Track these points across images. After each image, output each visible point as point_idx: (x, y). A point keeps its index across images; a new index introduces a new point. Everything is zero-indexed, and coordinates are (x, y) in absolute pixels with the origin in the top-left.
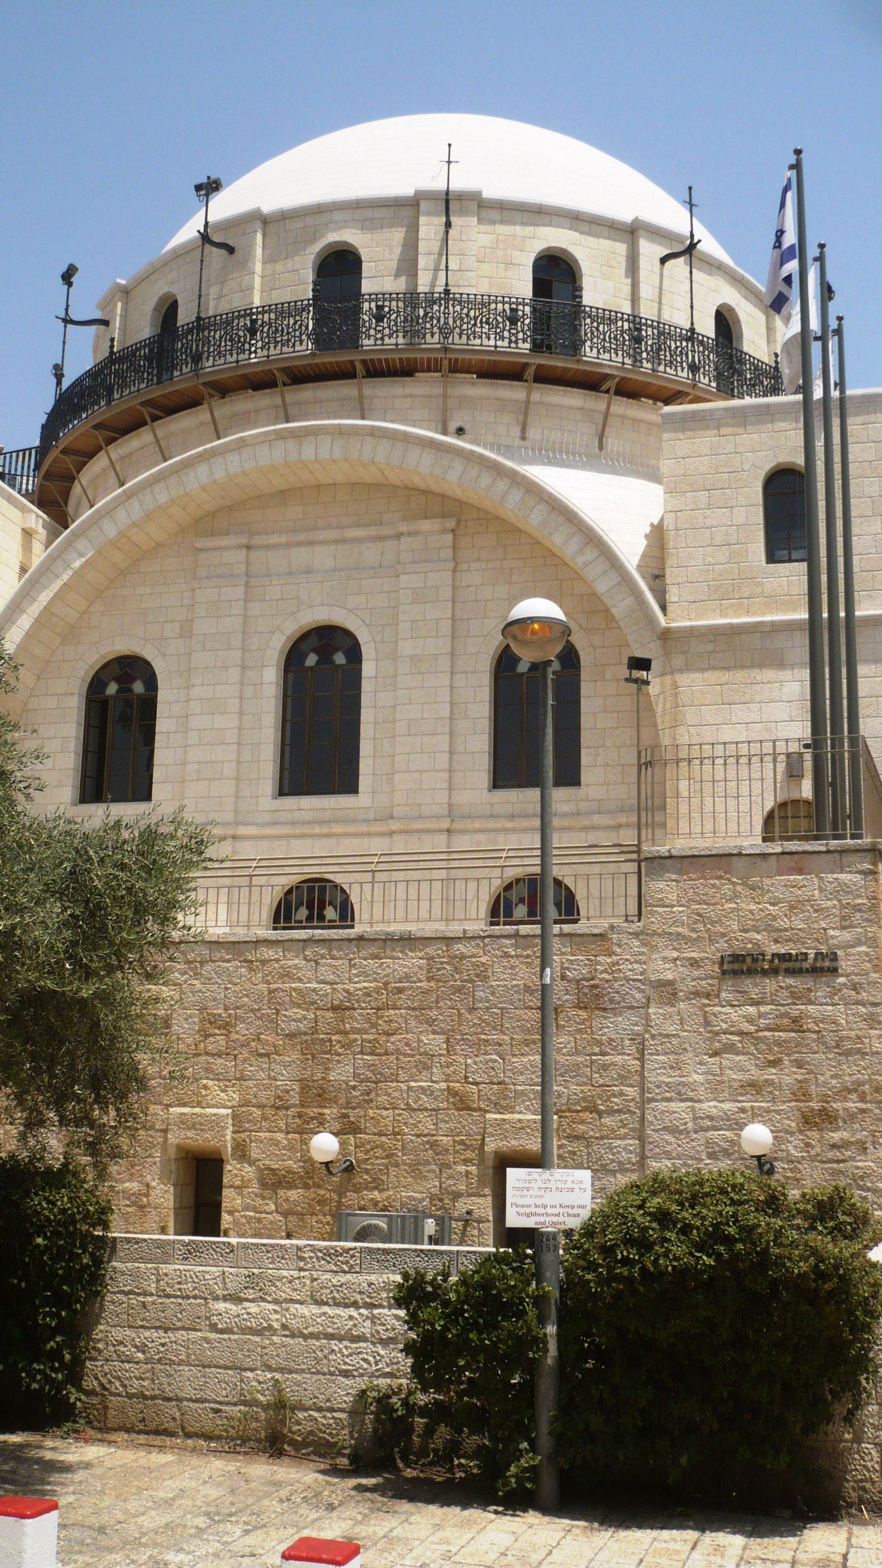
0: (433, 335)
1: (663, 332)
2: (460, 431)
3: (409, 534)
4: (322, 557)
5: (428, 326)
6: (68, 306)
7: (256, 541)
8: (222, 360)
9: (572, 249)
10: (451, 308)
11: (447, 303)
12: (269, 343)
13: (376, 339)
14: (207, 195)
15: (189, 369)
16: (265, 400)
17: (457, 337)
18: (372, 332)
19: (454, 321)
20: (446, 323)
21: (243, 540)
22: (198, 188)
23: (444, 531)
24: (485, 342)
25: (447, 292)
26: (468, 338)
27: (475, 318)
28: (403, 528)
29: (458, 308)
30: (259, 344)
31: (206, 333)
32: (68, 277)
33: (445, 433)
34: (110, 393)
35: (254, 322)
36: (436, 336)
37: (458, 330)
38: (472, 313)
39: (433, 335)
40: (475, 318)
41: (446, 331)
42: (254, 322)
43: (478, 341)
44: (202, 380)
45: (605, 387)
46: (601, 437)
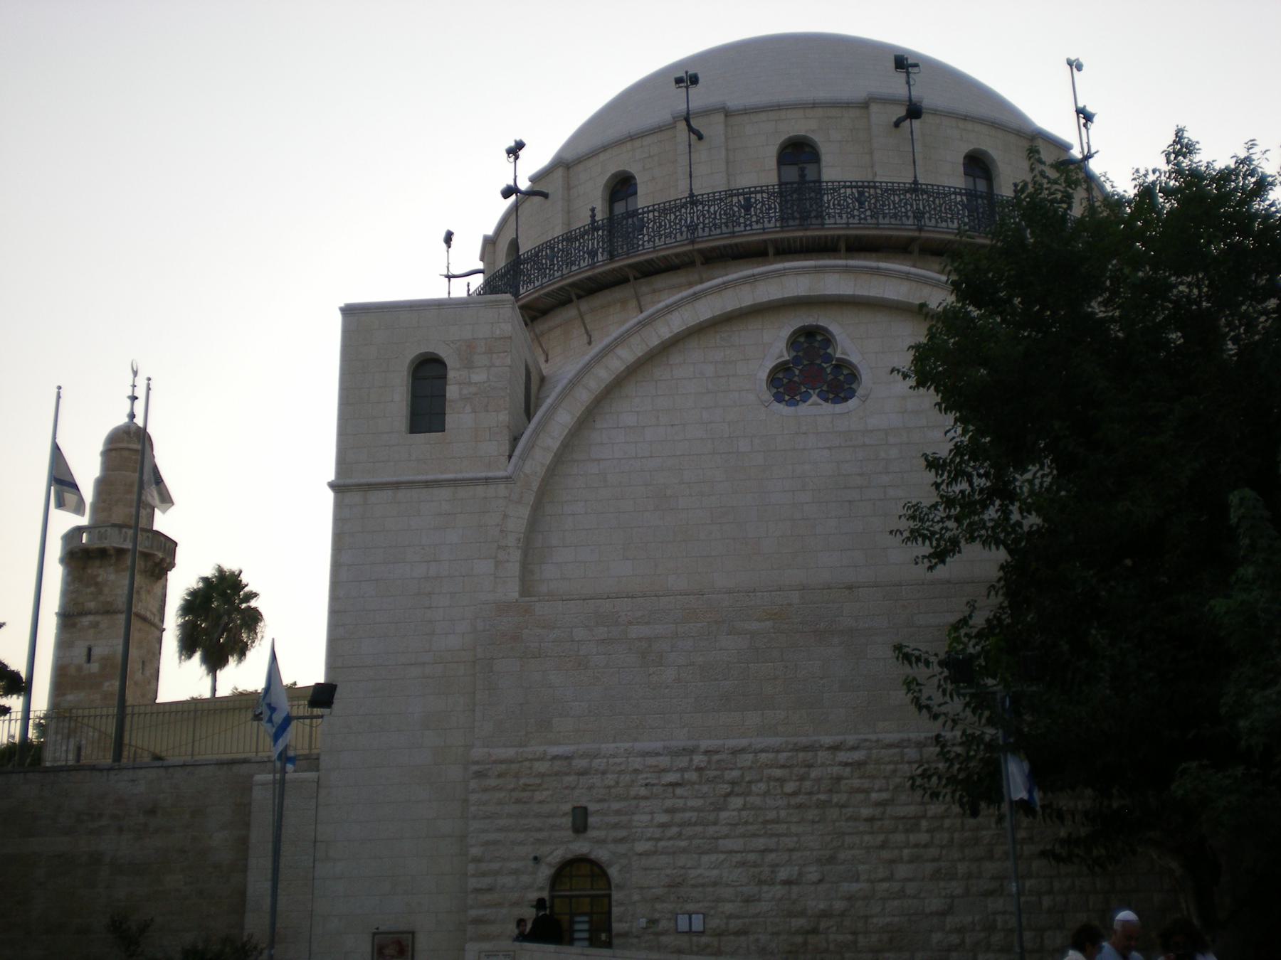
0: (908, 218)
8: (718, 231)
14: (687, 87)
15: (684, 236)
18: (856, 213)
22: (679, 81)
24: (950, 225)
25: (915, 182)
27: (940, 206)
30: (754, 219)
31: (700, 207)
32: (515, 150)
34: (593, 254)
35: (747, 200)
37: (927, 215)
39: (908, 218)
40: (940, 206)
41: (919, 215)
42: (747, 200)
43: (944, 224)
44: (697, 246)
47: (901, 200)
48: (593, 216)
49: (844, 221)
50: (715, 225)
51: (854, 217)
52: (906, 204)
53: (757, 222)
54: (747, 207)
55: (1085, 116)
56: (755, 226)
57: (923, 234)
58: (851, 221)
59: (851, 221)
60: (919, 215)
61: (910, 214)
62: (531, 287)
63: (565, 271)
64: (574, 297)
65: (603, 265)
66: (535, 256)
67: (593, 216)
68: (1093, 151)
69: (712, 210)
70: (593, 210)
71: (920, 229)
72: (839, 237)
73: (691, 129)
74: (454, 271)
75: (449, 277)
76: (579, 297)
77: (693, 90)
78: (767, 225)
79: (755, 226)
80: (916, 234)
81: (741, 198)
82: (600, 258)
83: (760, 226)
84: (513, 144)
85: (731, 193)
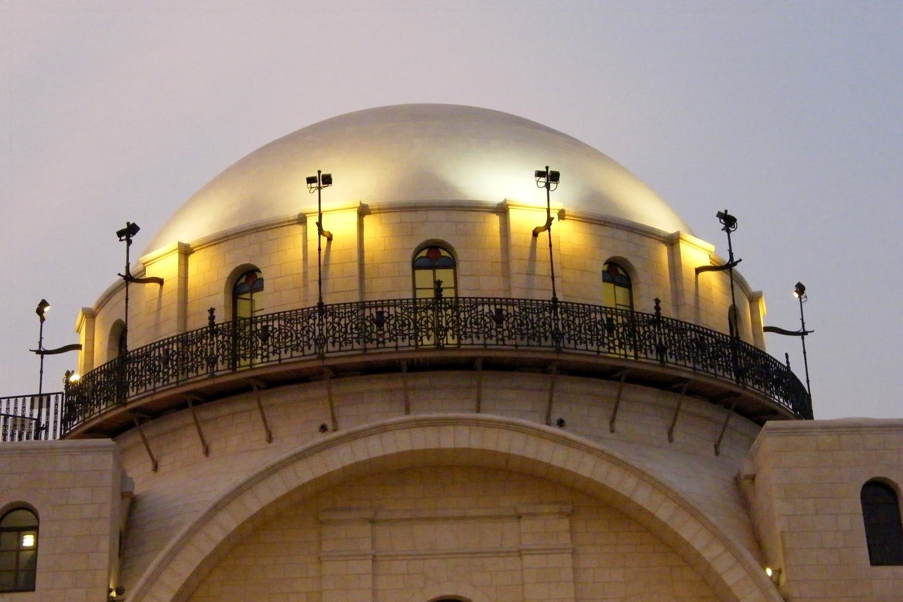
0: (546, 339)
1: (720, 341)
2: (561, 423)
3: (528, 514)
4: (447, 536)
5: (542, 330)
6: (128, 264)
7: (381, 515)
8: (349, 347)
9: (631, 260)
10: (559, 315)
11: (556, 310)
12: (397, 335)
13: (497, 340)
14: (319, 188)
15: (312, 350)
16: (379, 384)
17: (566, 341)
19: (563, 328)
20: (557, 329)
21: (369, 514)
22: (310, 180)
23: (561, 513)
25: (555, 299)
26: (576, 343)
28: (523, 510)
29: (565, 316)
30: (387, 335)
31: (330, 319)
33: (548, 424)
36: (550, 339)
37: (567, 335)
38: (577, 321)
39: (546, 339)
43: (583, 346)
45: (675, 386)
46: (670, 432)
47: (539, 320)
48: (212, 318)
49: (481, 341)
50: (345, 339)
51: (491, 337)
52: (544, 324)
53: (390, 339)
54: (380, 321)
55: (728, 221)
56: (388, 344)
57: (561, 357)
58: (488, 341)
59: (488, 341)
60: (557, 336)
61: (548, 334)
62: (142, 390)
63: (181, 378)
64: (190, 403)
65: (223, 372)
66: (145, 354)
67: (212, 318)
68: (735, 260)
69: (343, 322)
70: (212, 311)
71: (559, 351)
72: (475, 358)
73: (321, 232)
74: (47, 346)
75: (41, 352)
76: (196, 403)
77: (326, 191)
78: (400, 343)
79: (388, 344)
80: (555, 356)
81: (373, 311)
82: (220, 367)
83: (393, 344)
84: (125, 227)
85: (362, 305)
